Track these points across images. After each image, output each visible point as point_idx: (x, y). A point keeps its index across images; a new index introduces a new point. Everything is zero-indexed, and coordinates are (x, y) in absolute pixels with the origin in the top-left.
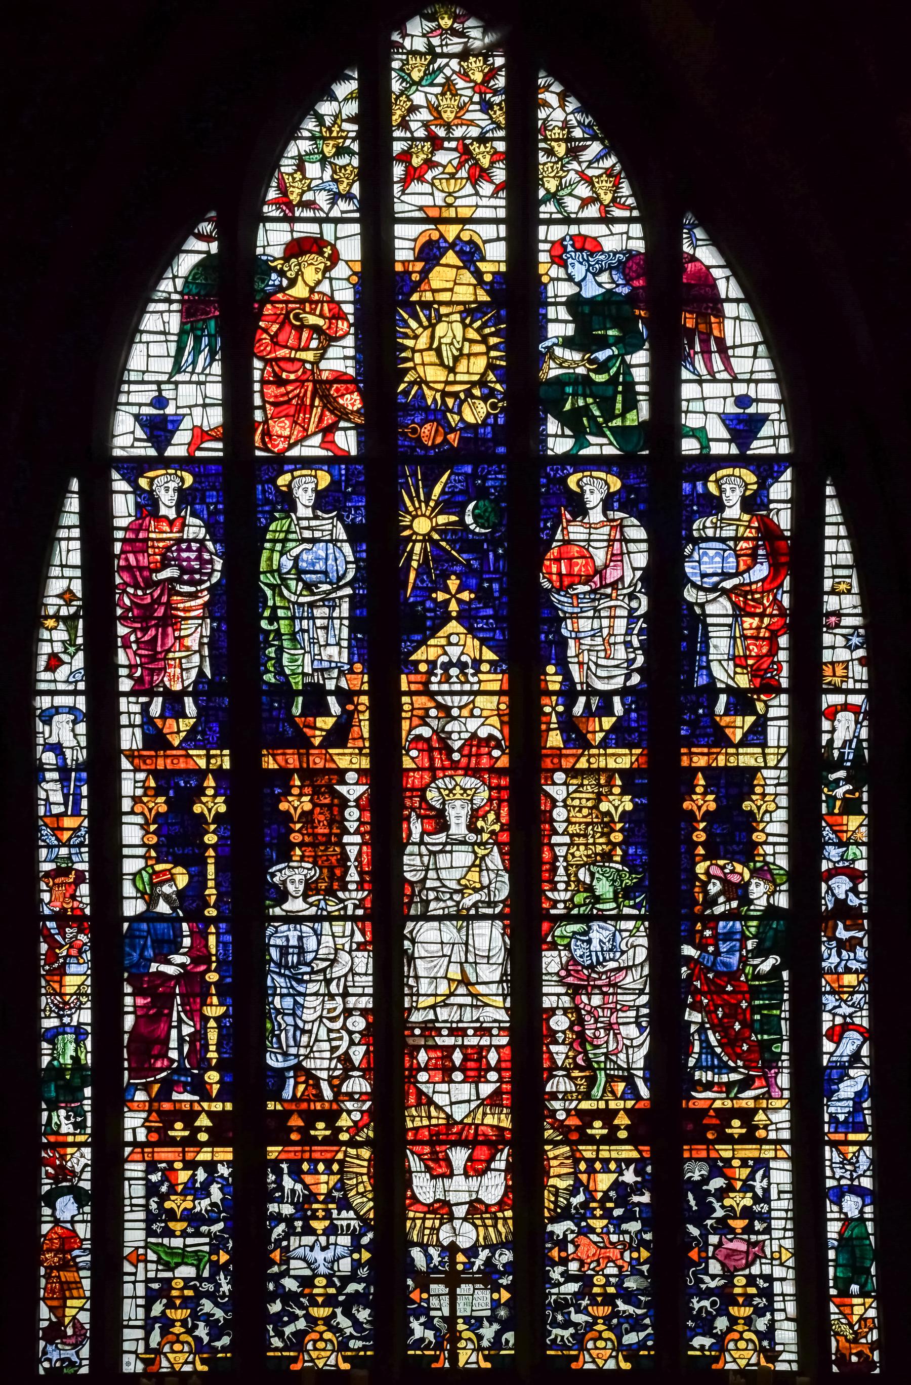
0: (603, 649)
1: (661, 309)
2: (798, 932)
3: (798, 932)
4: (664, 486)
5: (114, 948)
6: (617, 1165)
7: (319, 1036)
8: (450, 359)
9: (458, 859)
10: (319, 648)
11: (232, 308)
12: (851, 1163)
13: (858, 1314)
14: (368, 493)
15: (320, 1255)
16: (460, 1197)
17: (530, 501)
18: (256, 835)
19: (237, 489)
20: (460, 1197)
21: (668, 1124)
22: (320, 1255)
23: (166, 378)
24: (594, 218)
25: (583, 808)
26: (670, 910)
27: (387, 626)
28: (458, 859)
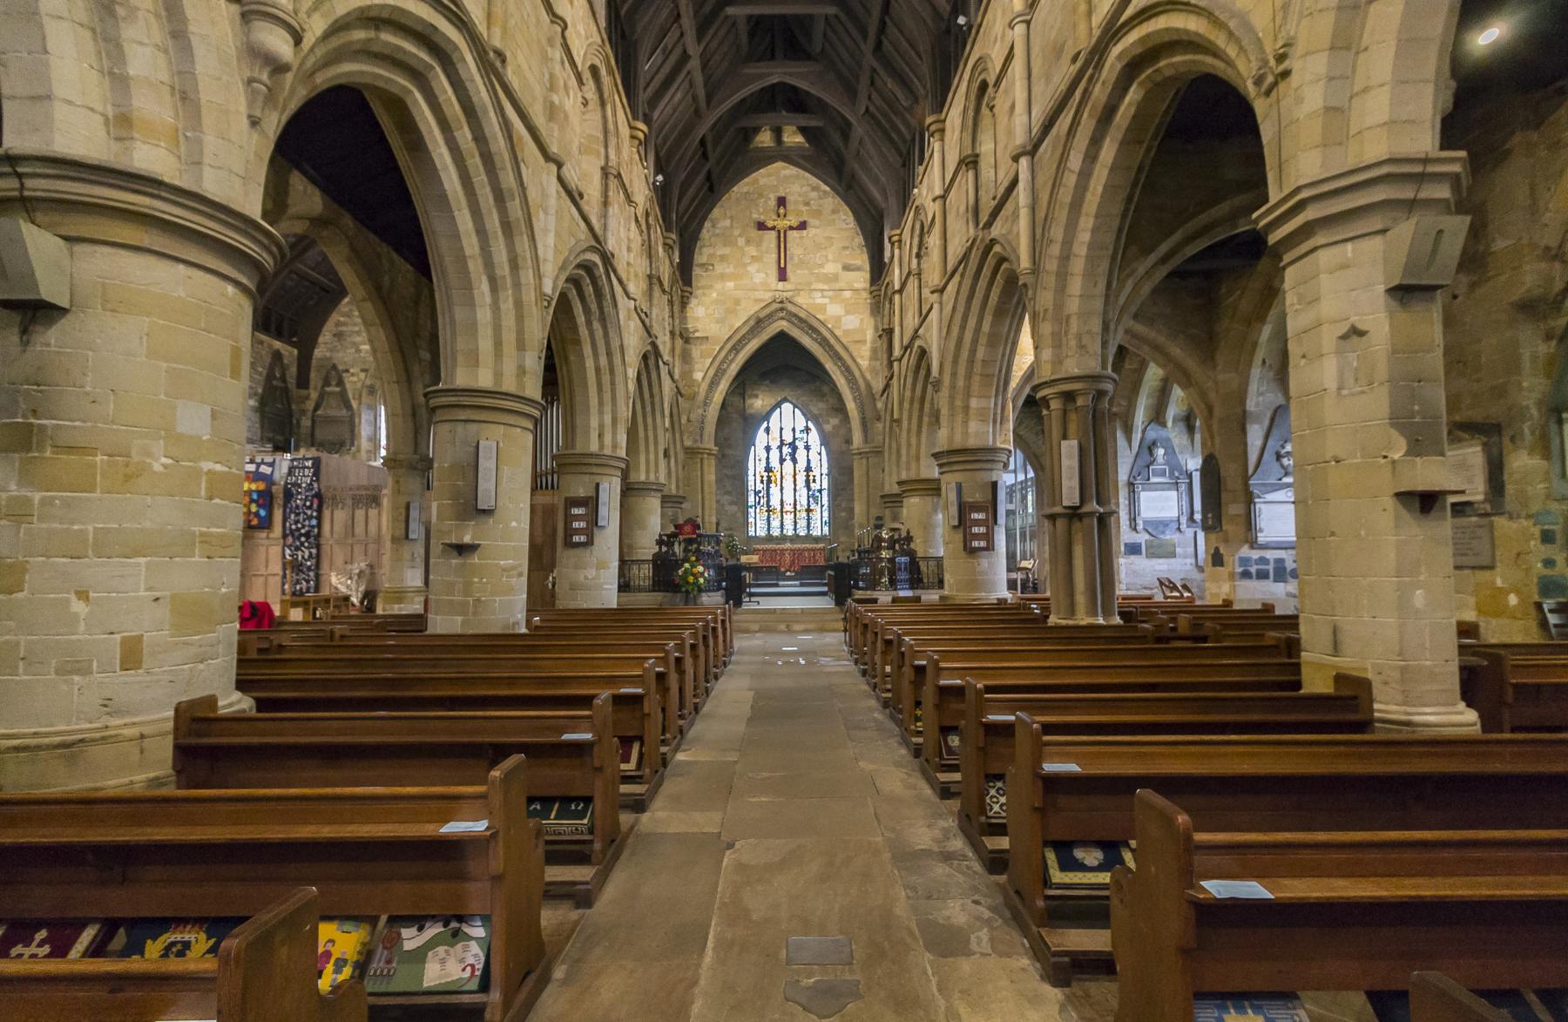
0: (802, 465)
1: (807, 429)
2: (820, 491)
3: (820, 491)
4: (807, 448)
5: (756, 493)
6: (804, 514)
7: (775, 502)
8: (788, 438)
9: (788, 484)
10: (775, 463)
11: (767, 430)
12: (826, 514)
13: (826, 529)
14: (780, 448)
15: (775, 523)
16: (788, 519)
17: (793, 446)
18: (769, 481)
19: (768, 449)
20: (788, 519)
21: (809, 510)
22: (775, 523)
23: (761, 434)
24: (801, 421)
25: (801, 478)
26: (809, 489)
27: (782, 461)
28: (788, 484)
